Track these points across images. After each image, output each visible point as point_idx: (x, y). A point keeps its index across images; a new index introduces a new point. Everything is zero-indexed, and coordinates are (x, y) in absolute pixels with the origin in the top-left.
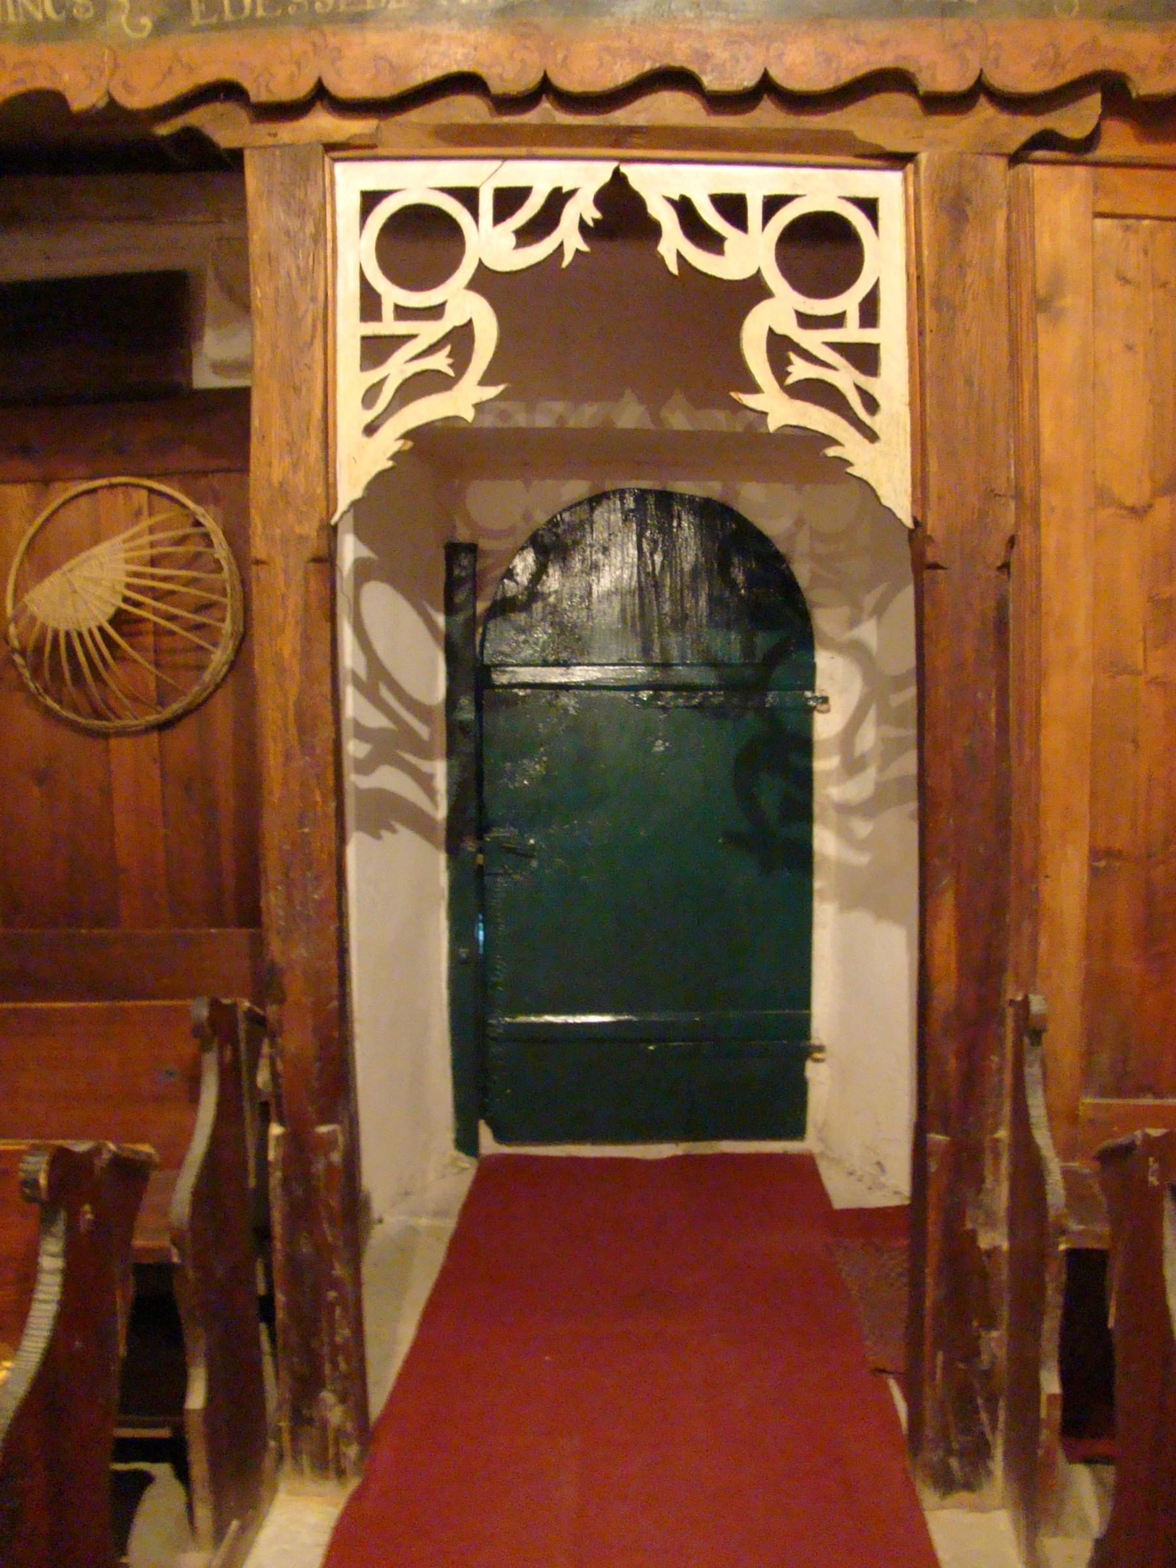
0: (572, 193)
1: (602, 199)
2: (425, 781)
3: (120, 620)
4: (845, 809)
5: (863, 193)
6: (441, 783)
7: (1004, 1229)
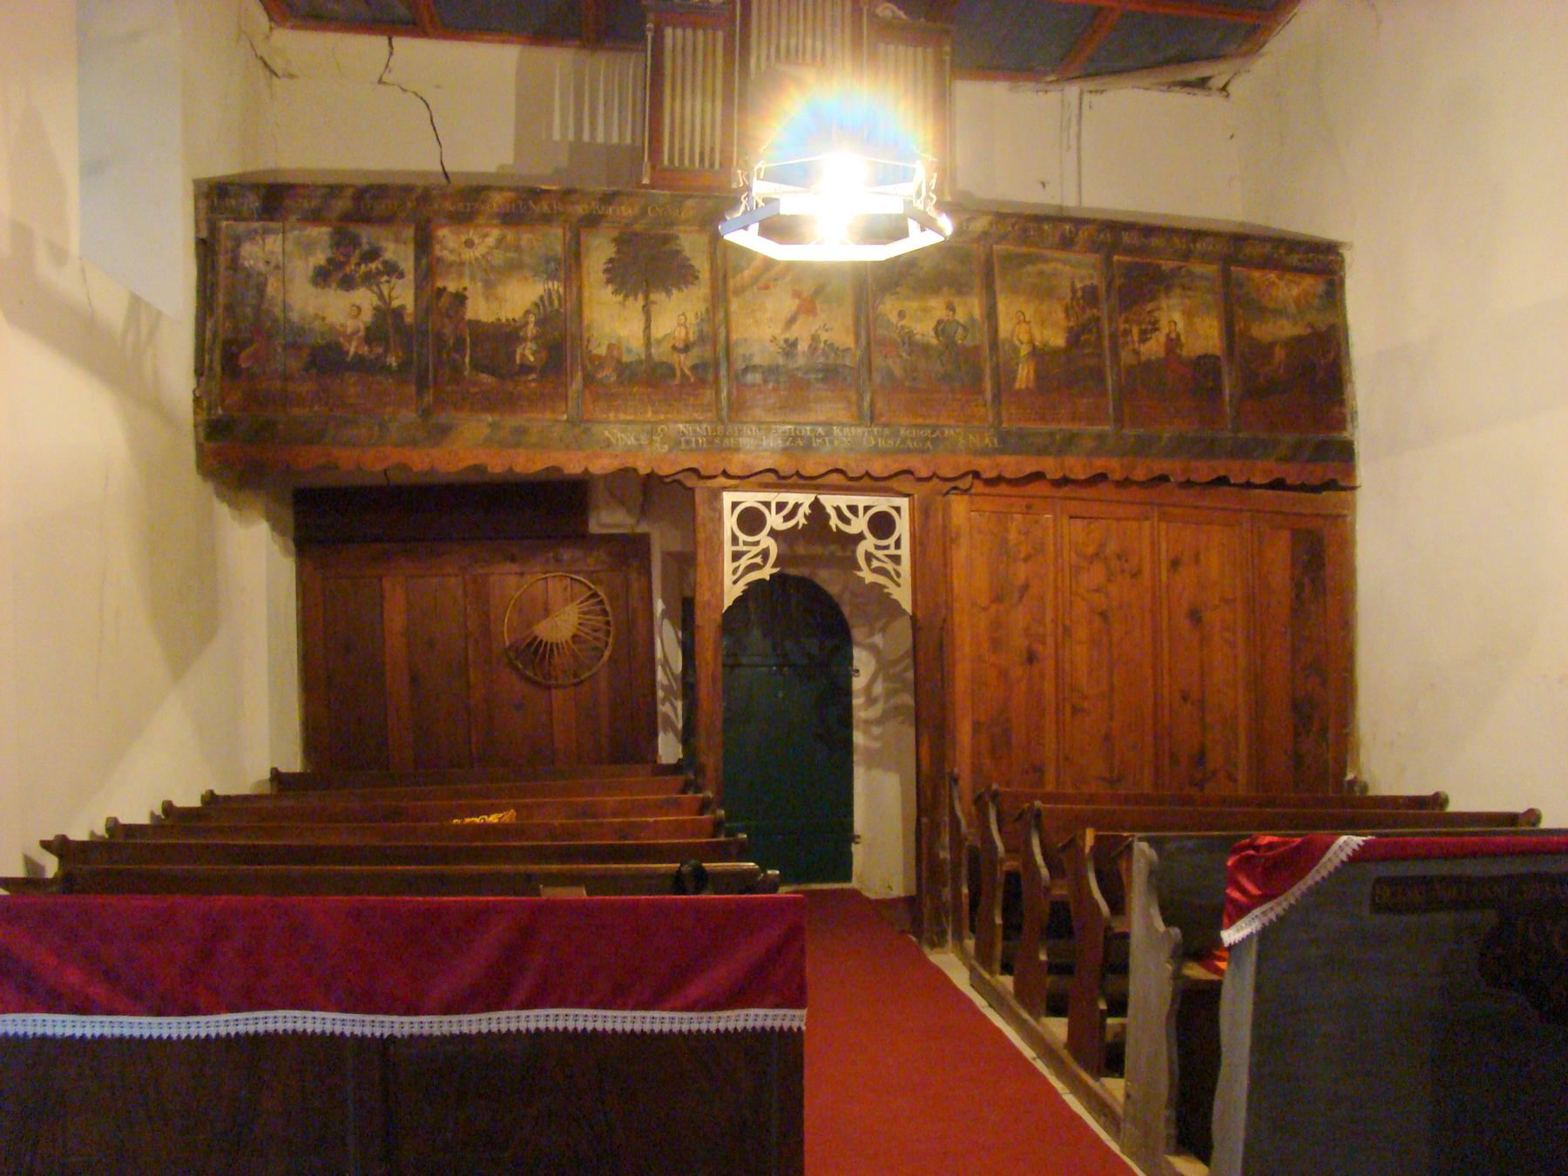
0: (801, 504)
1: (812, 506)
2: (675, 709)
3: (574, 636)
4: (867, 722)
5: (895, 505)
6: (680, 712)
7: (948, 851)
